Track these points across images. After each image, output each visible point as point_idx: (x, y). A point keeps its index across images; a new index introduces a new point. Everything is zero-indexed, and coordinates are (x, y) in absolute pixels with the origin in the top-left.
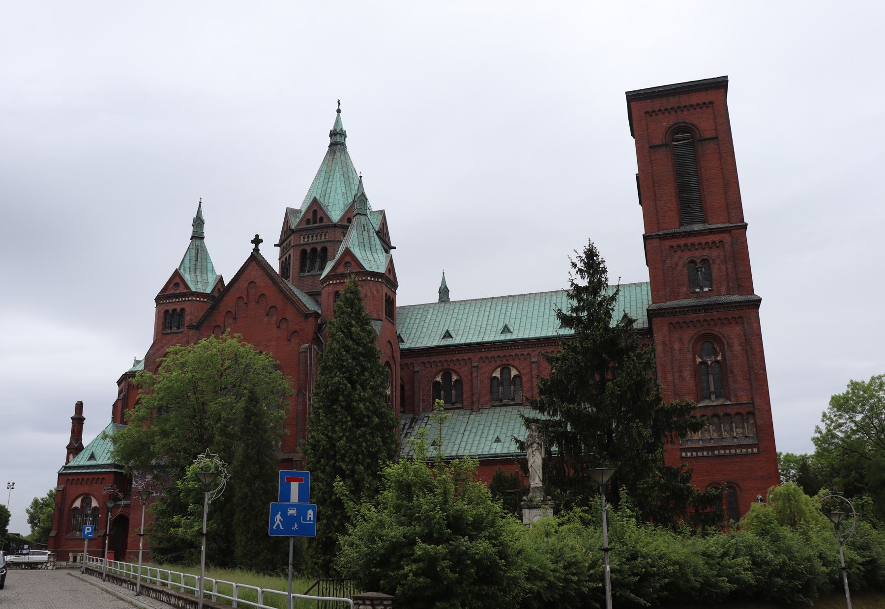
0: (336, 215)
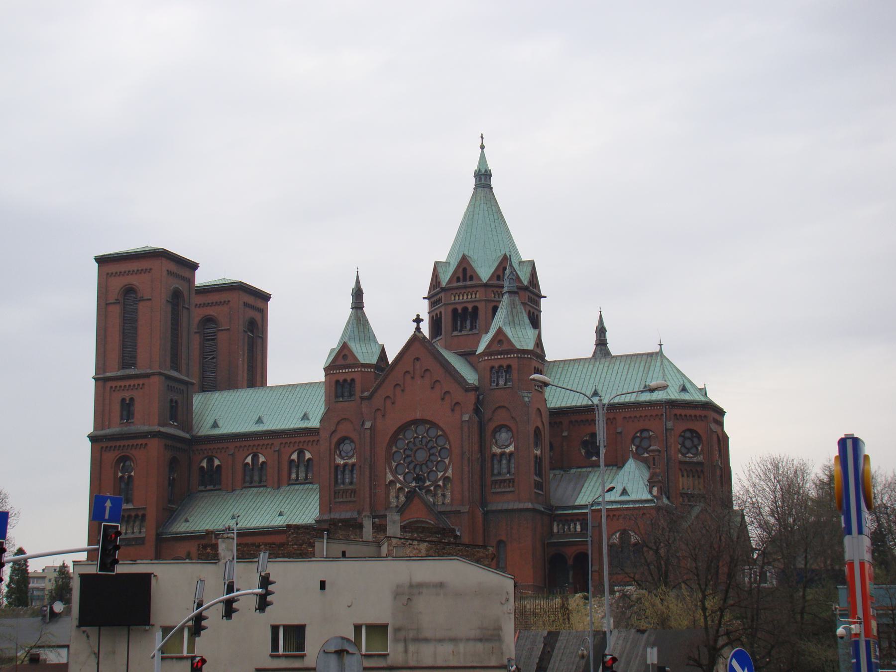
0: (485, 273)
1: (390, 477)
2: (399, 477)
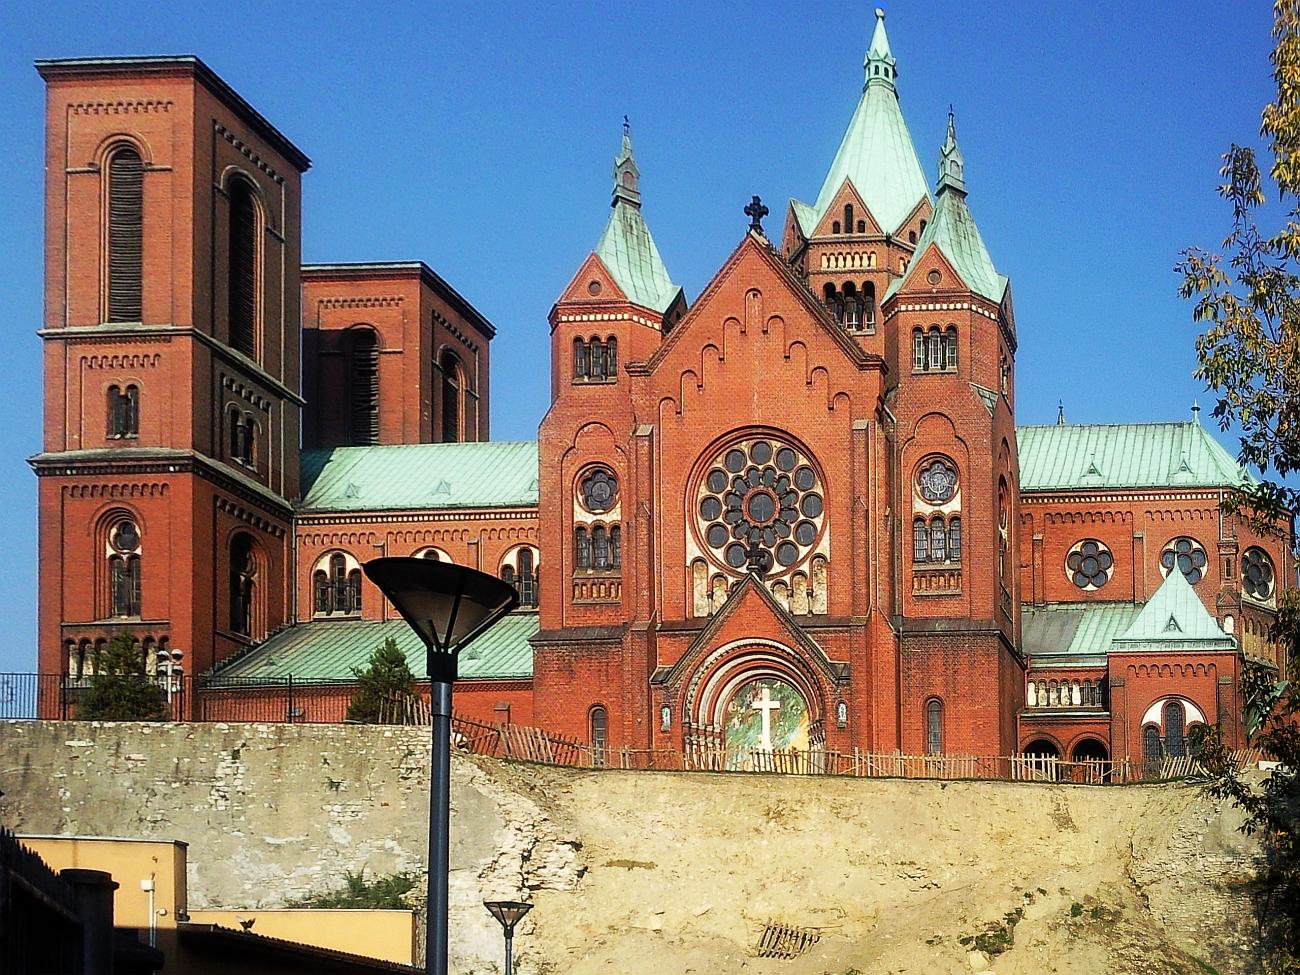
1: (693, 551)
2: (714, 551)
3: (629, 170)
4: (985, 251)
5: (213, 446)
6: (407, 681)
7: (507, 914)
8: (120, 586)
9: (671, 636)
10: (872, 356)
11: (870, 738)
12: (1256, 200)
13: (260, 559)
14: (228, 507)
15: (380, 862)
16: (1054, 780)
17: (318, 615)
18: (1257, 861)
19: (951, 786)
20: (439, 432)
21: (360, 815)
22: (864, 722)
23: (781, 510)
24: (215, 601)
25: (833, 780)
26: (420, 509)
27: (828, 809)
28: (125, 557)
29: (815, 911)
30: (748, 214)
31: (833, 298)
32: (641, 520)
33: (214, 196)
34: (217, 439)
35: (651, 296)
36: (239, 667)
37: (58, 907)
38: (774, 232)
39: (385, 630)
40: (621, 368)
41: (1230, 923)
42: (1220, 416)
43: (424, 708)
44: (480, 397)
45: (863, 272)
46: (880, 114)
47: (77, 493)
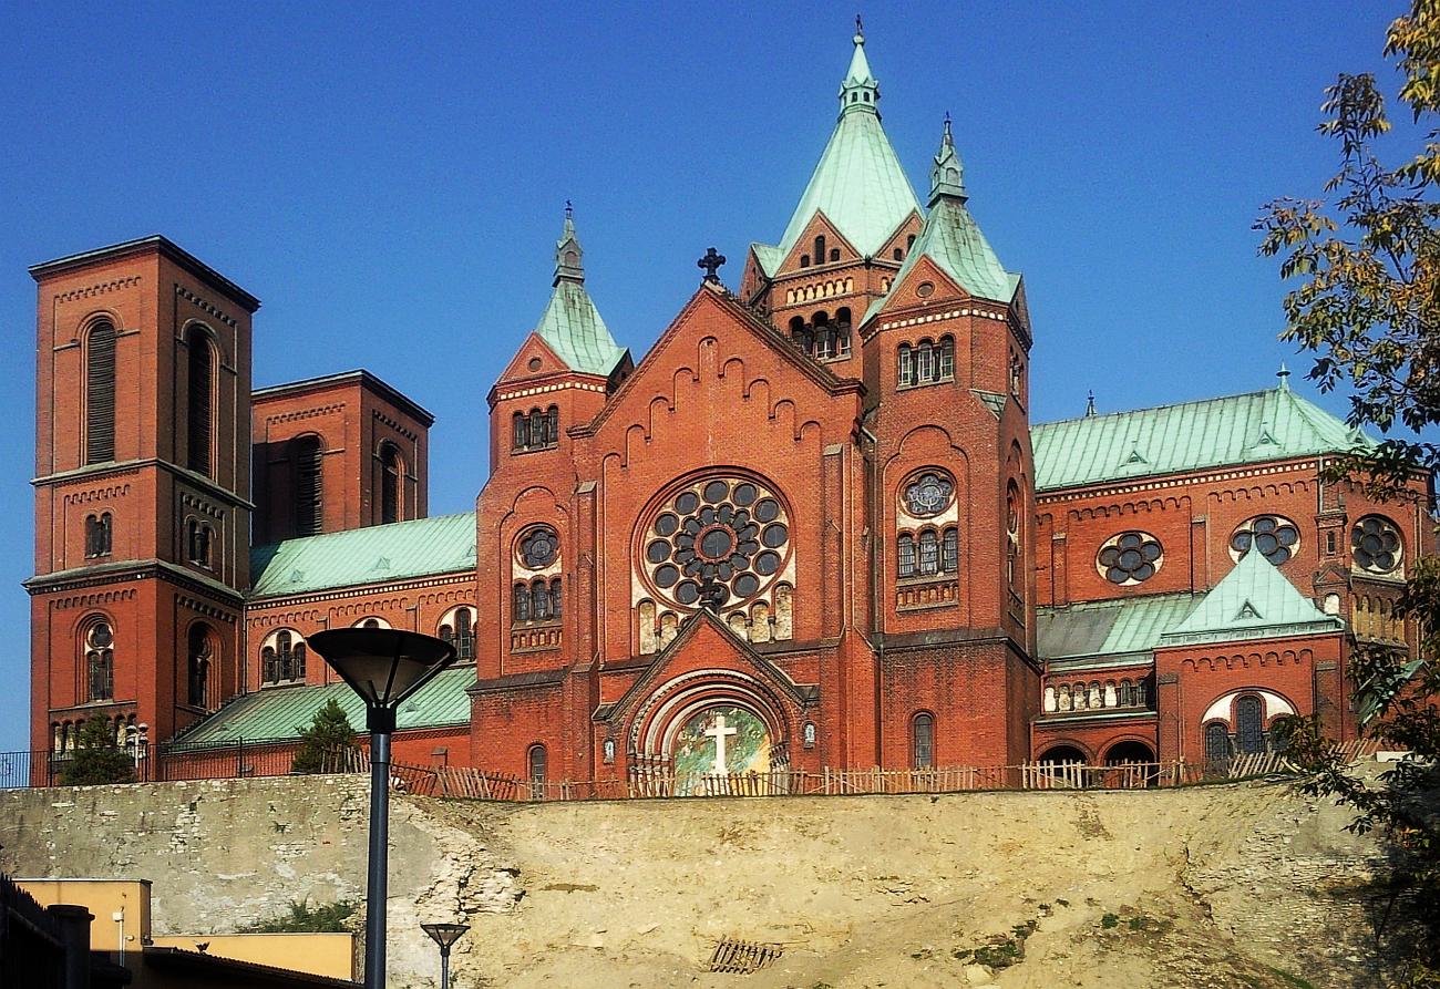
1: (639, 593)
2: (663, 591)
3: (571, 249)
4: (990, 253)
5: (174, 554)
6: (348, 736)
7: (444, 935)
8: (96, 676)
9: (615, 674)
10: (847, 381)
11: (843, 756)
12: (1377, 129)
13: (214, 643)
14: (186, 603)
15: (322, 892)
16: (1080, 786)
17: (265, 685)
18: (1373, 864)
19: (944, 799)
20: (379, 515)
21: (304, 852)
22: (836, 741)
23: (739, 544)
24: (175, 681)
25: (798, 800)
26: (360, 585)
27: (792, 828)
28: (100, 653)
29: (776, 927)
30: (702, 266)
31: (801, 330)
32: (583, 570)
33: (175, 347)
34: (178, 547)
35: (595, 362)
36: (195, 734)
37: (45, 935)
38: (733, 279)
39: (328, 692)
40: (562, 434)
41: (1332, 933)
42: (1320, 377)
43: (364, 757)
44: (418, 481)
45: (837, 299)
46: (859, 140)
47: (62, 605)
